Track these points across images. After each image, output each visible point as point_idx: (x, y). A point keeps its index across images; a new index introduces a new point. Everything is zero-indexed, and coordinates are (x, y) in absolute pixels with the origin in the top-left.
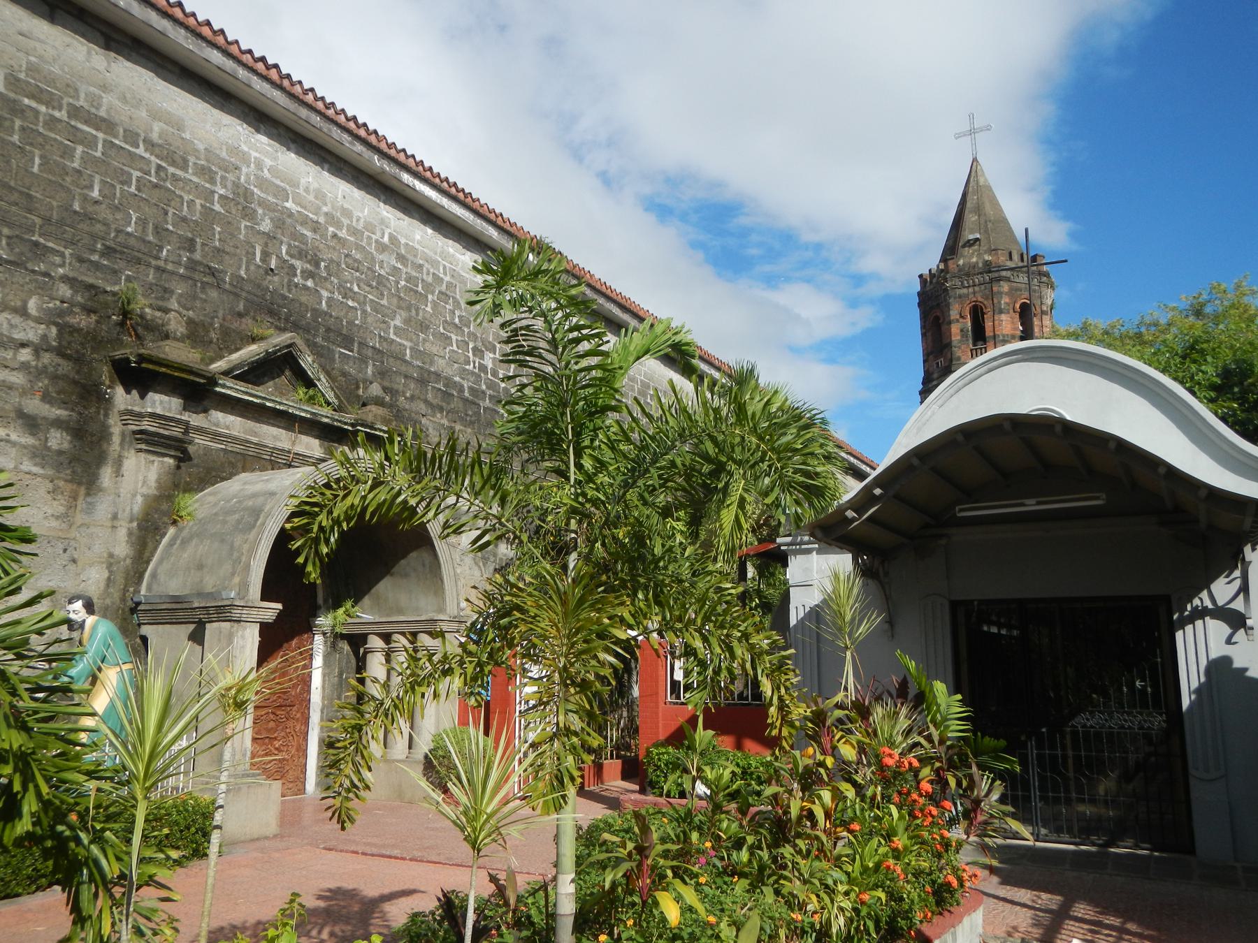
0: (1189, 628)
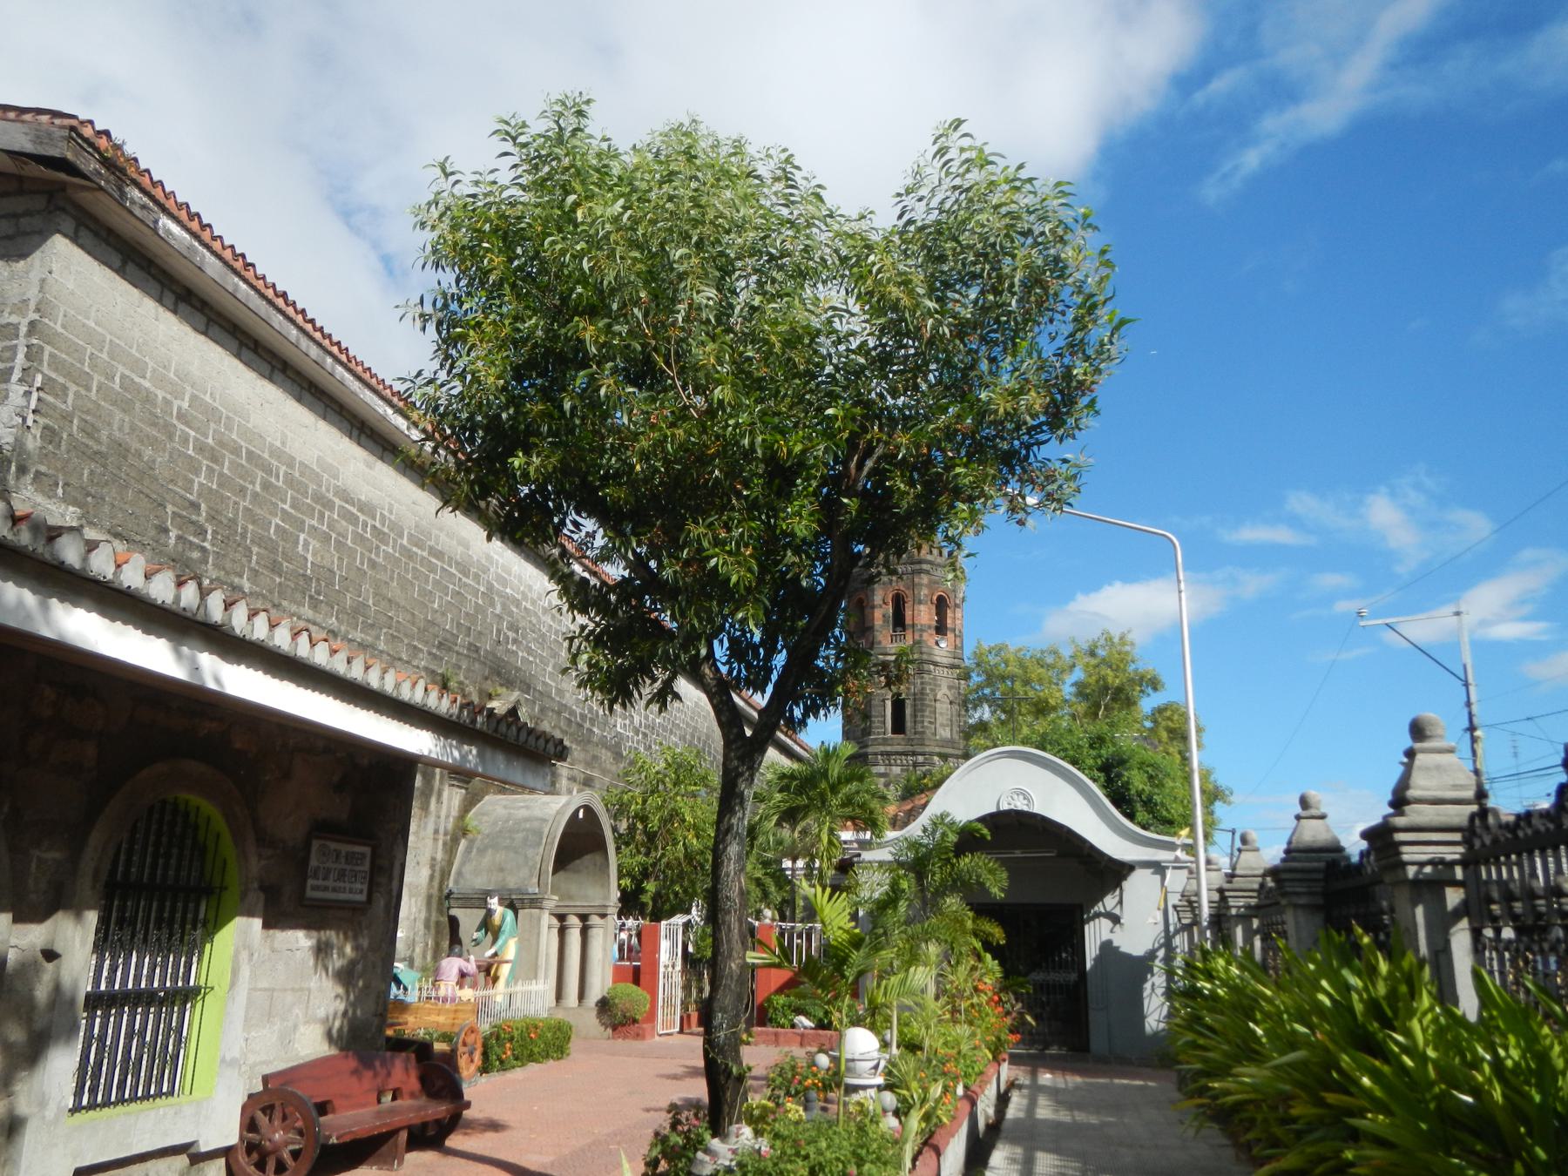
0: (1092, 923)
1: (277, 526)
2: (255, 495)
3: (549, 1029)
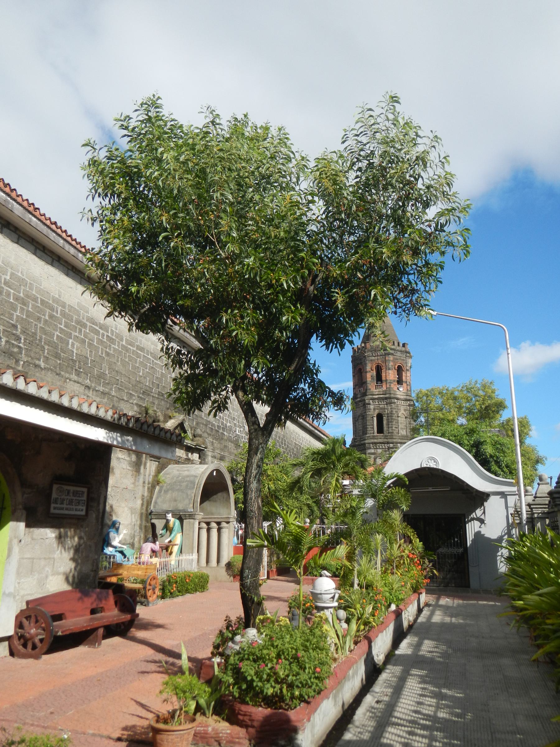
0: (470, 523)
1: (57, 335)
2: (46, 321)
3: (196, 577)
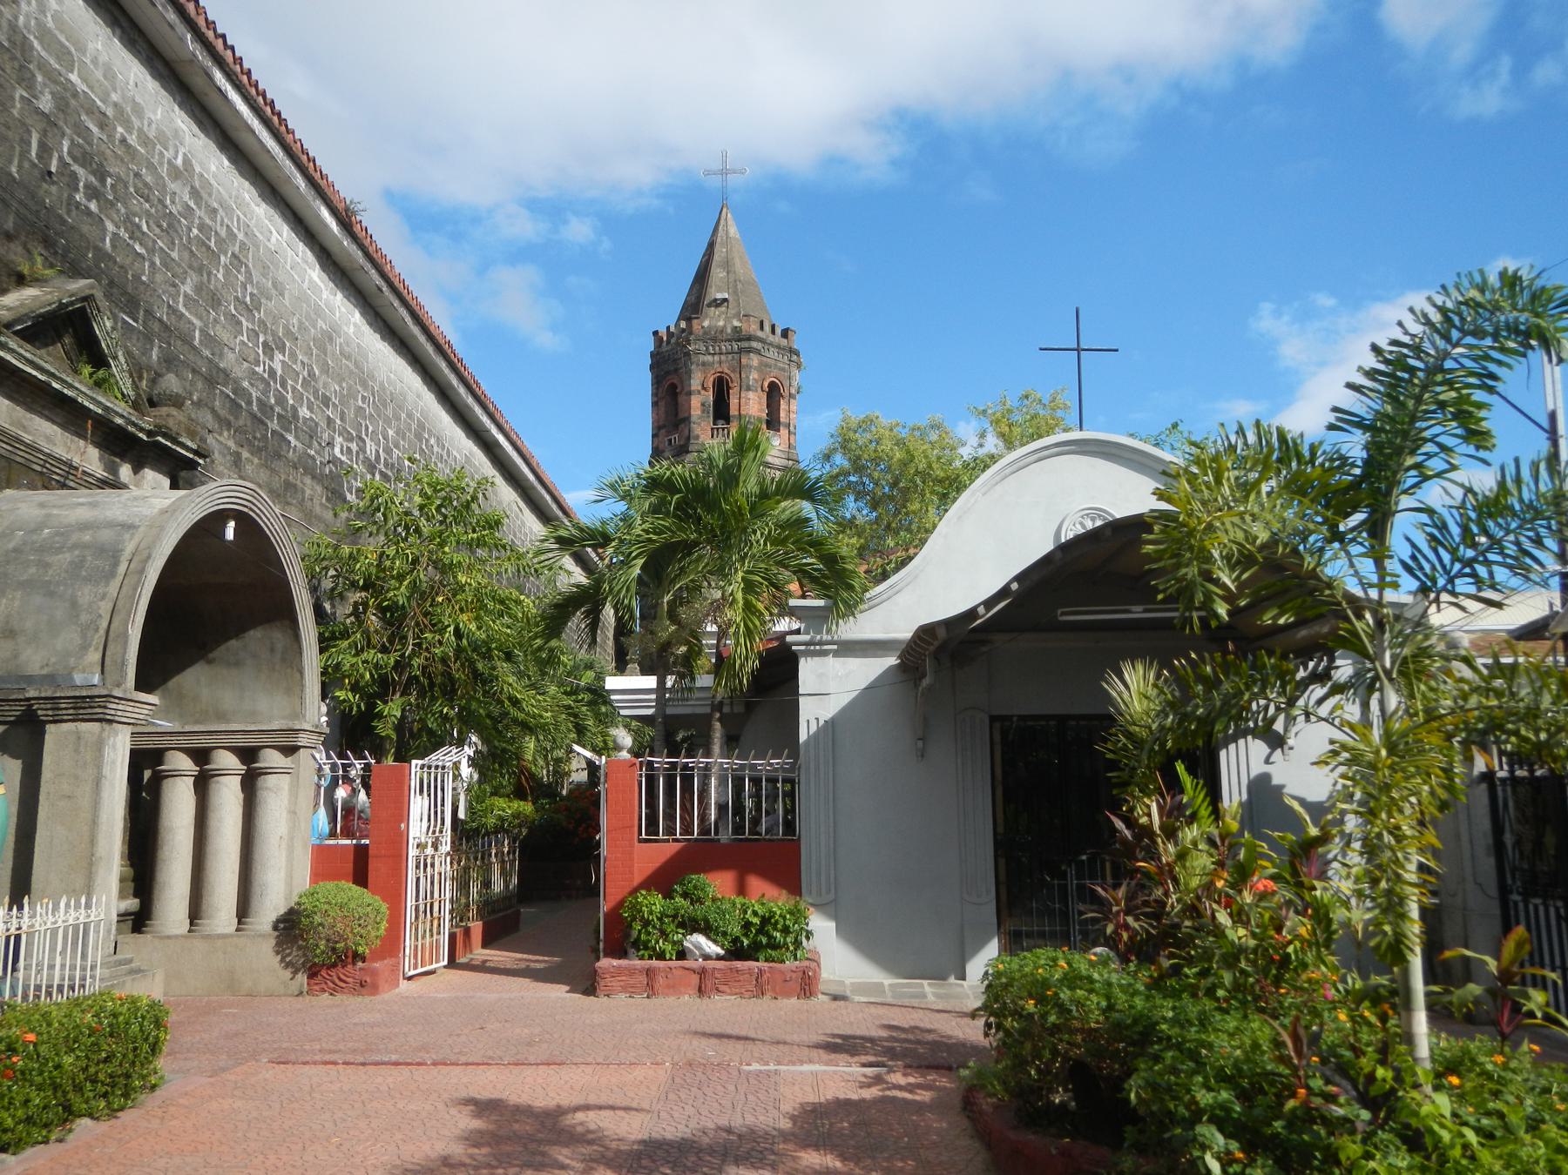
0: (1232, 747)
